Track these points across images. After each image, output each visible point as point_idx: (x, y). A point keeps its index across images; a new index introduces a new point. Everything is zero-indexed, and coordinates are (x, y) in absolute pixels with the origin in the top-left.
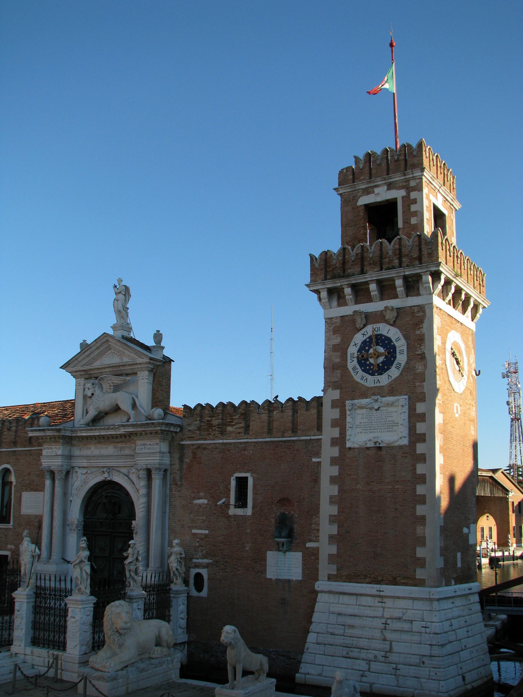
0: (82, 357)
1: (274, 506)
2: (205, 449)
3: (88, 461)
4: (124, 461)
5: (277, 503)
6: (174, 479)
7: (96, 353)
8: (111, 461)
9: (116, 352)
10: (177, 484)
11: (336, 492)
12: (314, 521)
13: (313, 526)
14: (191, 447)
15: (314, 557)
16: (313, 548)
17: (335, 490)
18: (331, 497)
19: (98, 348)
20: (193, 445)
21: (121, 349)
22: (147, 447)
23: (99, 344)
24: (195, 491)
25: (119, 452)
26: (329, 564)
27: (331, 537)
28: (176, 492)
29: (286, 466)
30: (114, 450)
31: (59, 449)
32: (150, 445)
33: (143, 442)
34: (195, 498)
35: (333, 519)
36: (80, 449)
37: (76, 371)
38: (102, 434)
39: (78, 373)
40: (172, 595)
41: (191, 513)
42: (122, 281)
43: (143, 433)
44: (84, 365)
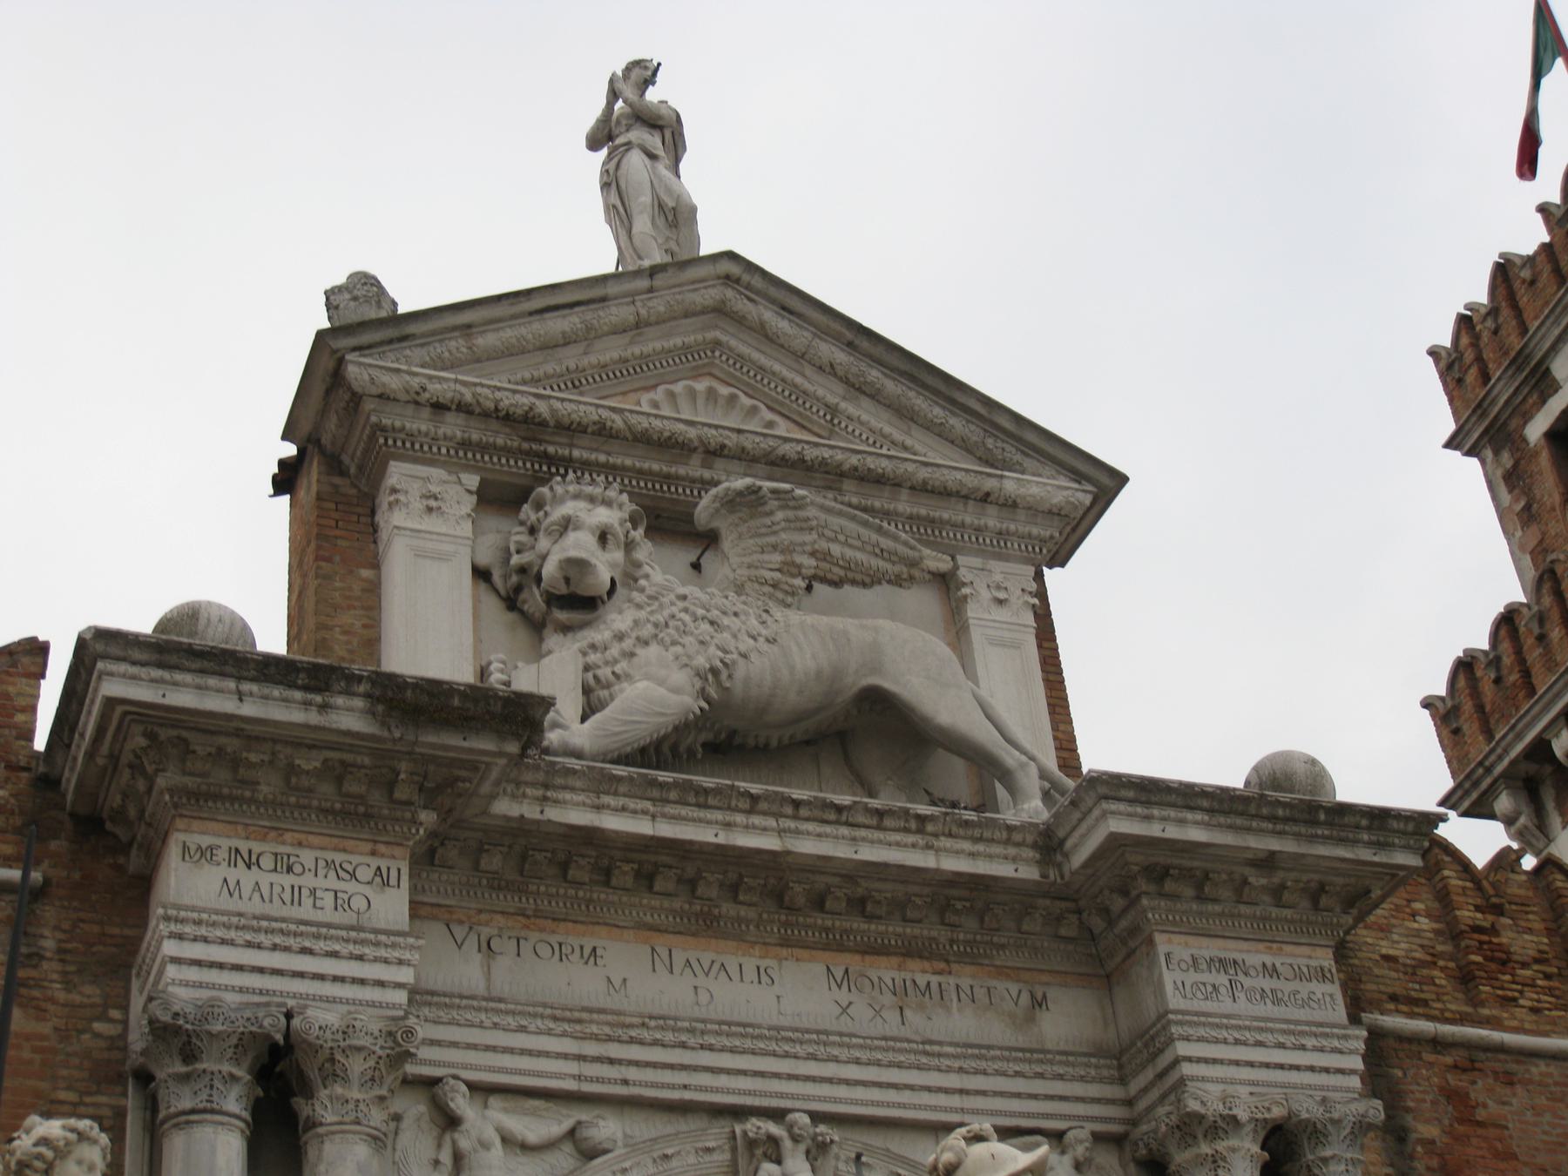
0: (509, 334)
2: (1509, 1080)
3: (591, 1049)
4: (953, 1081)
7: (610, 351)
8: (829, 1070)
9: (746, 401)
14: (1428, 1057)
19: (639, 325)
20: (1437, 1043)
21: (828, 391)
22: (1247, 982)
23: (659, 305)
25: (892, 1016)
30: (843, 996)
31: (382, 879)
32: (1273, 972)
33: (1210, 948)
36: (488, 948)
37: (439, 407)
38: (807, 846)
39: (453, 426)
42: (650, 81)
43: (1258, 880)
44: (366, 412)
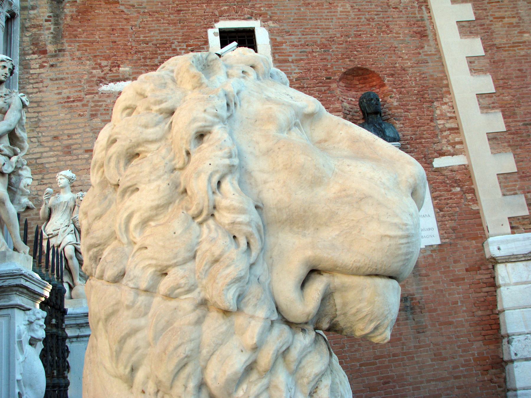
1: (334, 86)
5: (341, 79)
6: (35, 42)
10: (44, 52)
11: (481, 52)
12: (438, 112)
13: (439, 122)
15: (458, 189)
16: (452, 170)
17: (476, 46)
18: (471, 61)
24: (104, 63)
26: (504, 195)
27: (494, 138)
28: (42, 70)
29: (348, 6)
34: (102, 80)
35: (487, 102)
40: (70, 332)
41: (93, 116)
